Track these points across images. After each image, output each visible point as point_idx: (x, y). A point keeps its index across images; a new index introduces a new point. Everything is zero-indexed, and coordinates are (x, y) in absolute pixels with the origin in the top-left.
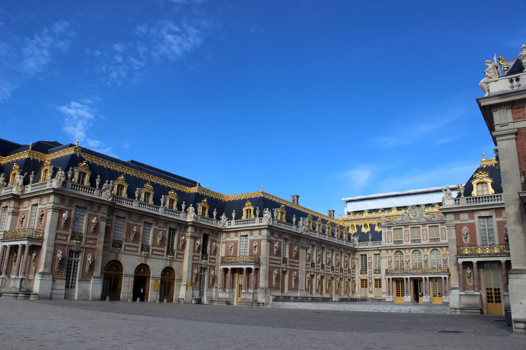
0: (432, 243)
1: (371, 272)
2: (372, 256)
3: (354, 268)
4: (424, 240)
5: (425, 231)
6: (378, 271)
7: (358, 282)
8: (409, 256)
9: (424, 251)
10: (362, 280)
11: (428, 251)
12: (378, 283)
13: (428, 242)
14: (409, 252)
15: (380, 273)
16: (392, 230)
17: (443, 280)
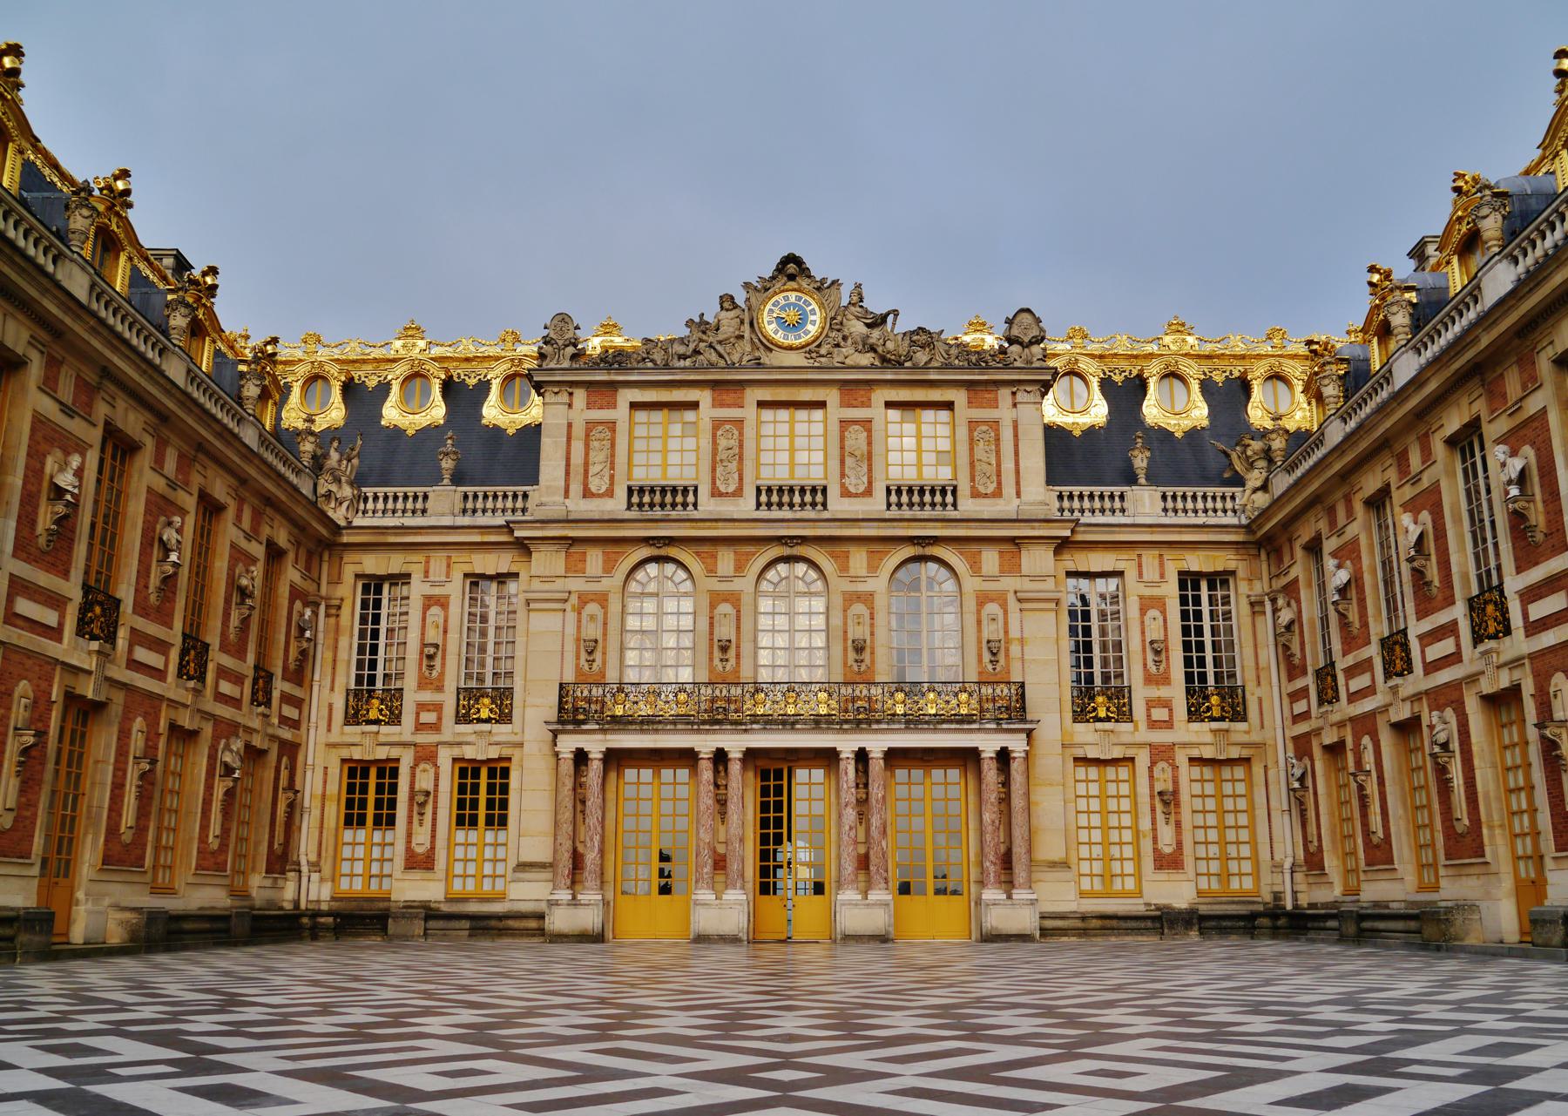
0: (906, 513)
1: (438, 708)
2: (455, 589)
3: (299, 673)
4: (846, 493)
5: (857, 439)
6: (490, 699)
7: (320, 779)
8: (734, 599)
9: (844, 568)
10: (356, 771)
11: (873, 568)
12: (484, 793)
13: (876, 505)
14: (740, 568)
15: (505, 717)
16: (621, 413)
17: (990, 773)
